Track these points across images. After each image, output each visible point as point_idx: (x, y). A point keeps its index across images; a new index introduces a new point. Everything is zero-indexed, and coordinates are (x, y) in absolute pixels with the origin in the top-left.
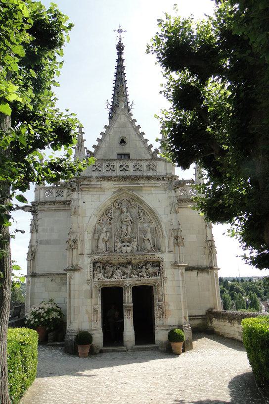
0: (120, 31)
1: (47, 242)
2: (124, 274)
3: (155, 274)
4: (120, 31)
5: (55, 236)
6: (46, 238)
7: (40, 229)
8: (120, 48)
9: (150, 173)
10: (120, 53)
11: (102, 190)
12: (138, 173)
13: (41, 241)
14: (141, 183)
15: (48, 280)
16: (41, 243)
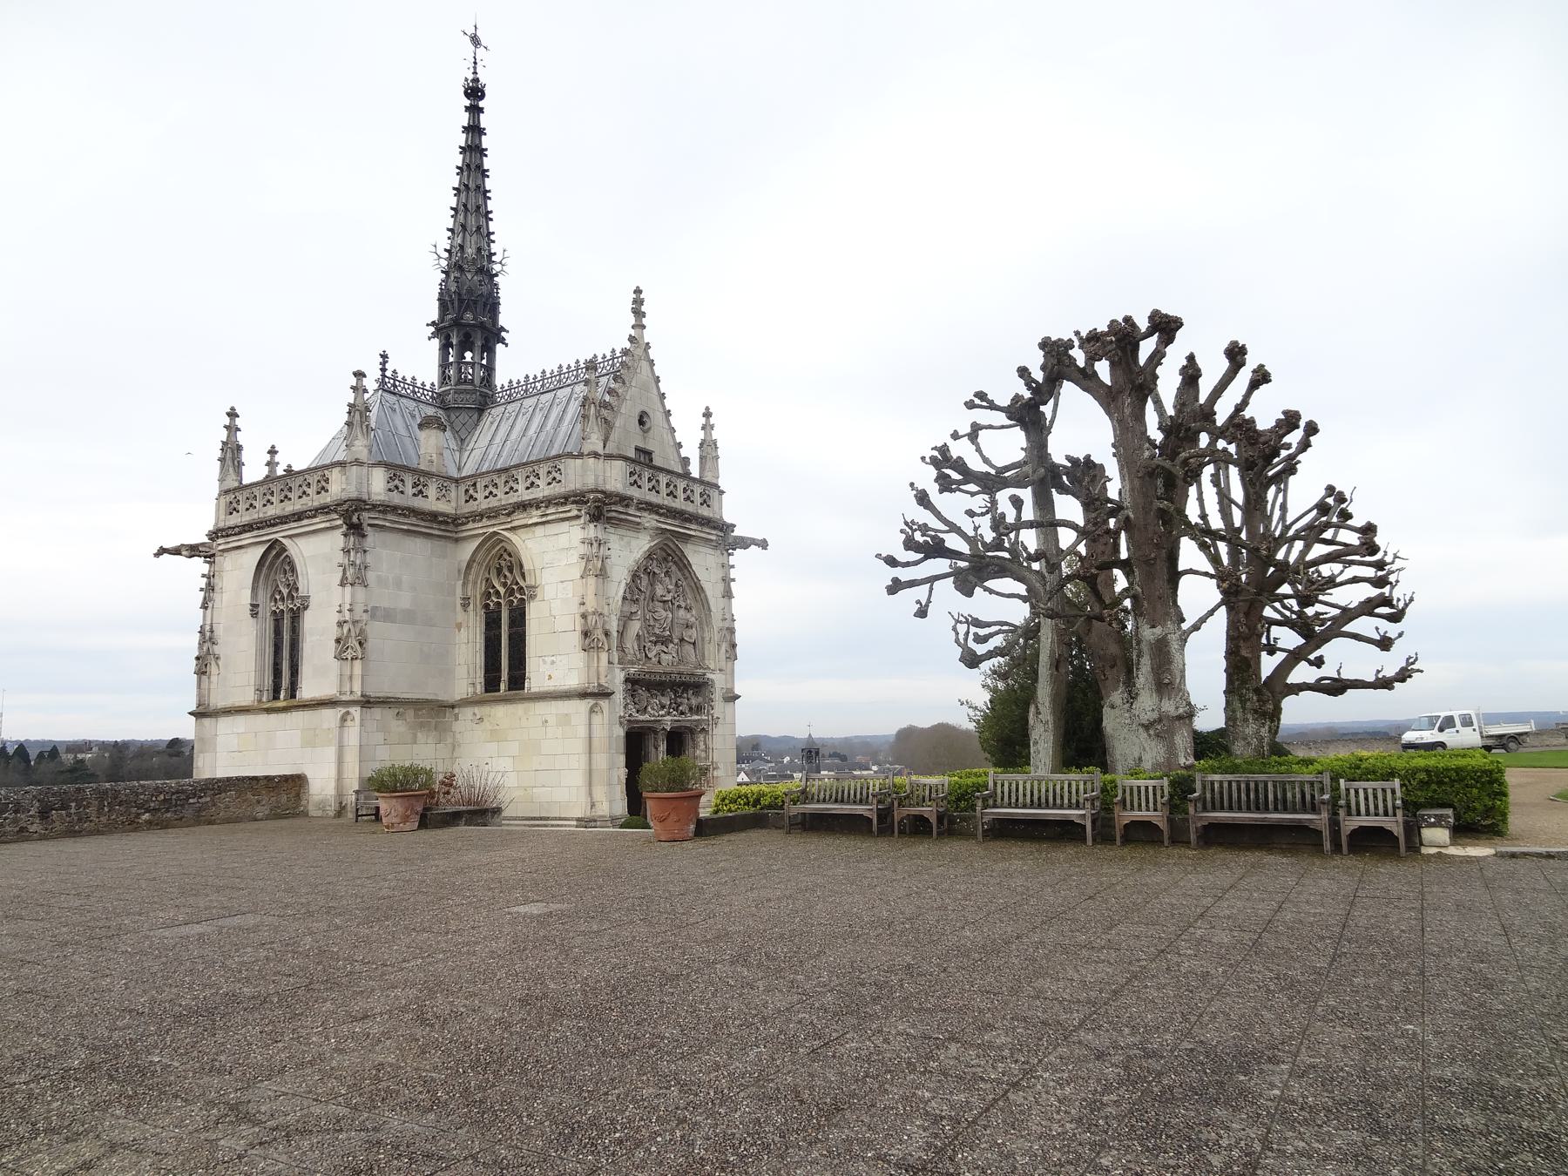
0: (475, 41)
1: (388, 616)
2: (663, 707)
3: (699, 709)
4: (475, 41)
5: (404, 601)
6: (385, 604)
7: (371, 576)
8: (475, 92)
9: (704, 512)
10: (475, 110)
11: (636, 527)
12: (690, 508)
13: (375, 608)
14: (693, 530)
15: (389, 714)
16: (373, 617)
